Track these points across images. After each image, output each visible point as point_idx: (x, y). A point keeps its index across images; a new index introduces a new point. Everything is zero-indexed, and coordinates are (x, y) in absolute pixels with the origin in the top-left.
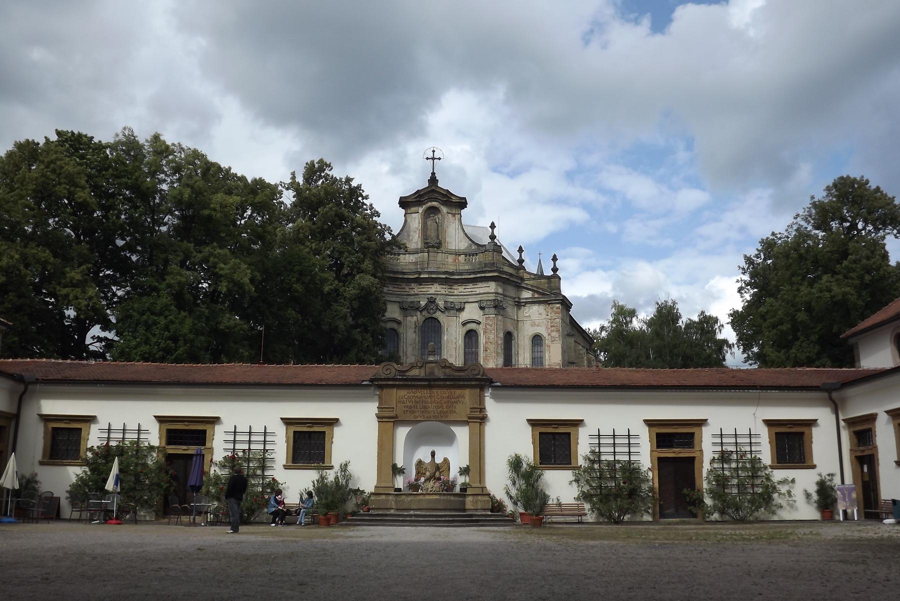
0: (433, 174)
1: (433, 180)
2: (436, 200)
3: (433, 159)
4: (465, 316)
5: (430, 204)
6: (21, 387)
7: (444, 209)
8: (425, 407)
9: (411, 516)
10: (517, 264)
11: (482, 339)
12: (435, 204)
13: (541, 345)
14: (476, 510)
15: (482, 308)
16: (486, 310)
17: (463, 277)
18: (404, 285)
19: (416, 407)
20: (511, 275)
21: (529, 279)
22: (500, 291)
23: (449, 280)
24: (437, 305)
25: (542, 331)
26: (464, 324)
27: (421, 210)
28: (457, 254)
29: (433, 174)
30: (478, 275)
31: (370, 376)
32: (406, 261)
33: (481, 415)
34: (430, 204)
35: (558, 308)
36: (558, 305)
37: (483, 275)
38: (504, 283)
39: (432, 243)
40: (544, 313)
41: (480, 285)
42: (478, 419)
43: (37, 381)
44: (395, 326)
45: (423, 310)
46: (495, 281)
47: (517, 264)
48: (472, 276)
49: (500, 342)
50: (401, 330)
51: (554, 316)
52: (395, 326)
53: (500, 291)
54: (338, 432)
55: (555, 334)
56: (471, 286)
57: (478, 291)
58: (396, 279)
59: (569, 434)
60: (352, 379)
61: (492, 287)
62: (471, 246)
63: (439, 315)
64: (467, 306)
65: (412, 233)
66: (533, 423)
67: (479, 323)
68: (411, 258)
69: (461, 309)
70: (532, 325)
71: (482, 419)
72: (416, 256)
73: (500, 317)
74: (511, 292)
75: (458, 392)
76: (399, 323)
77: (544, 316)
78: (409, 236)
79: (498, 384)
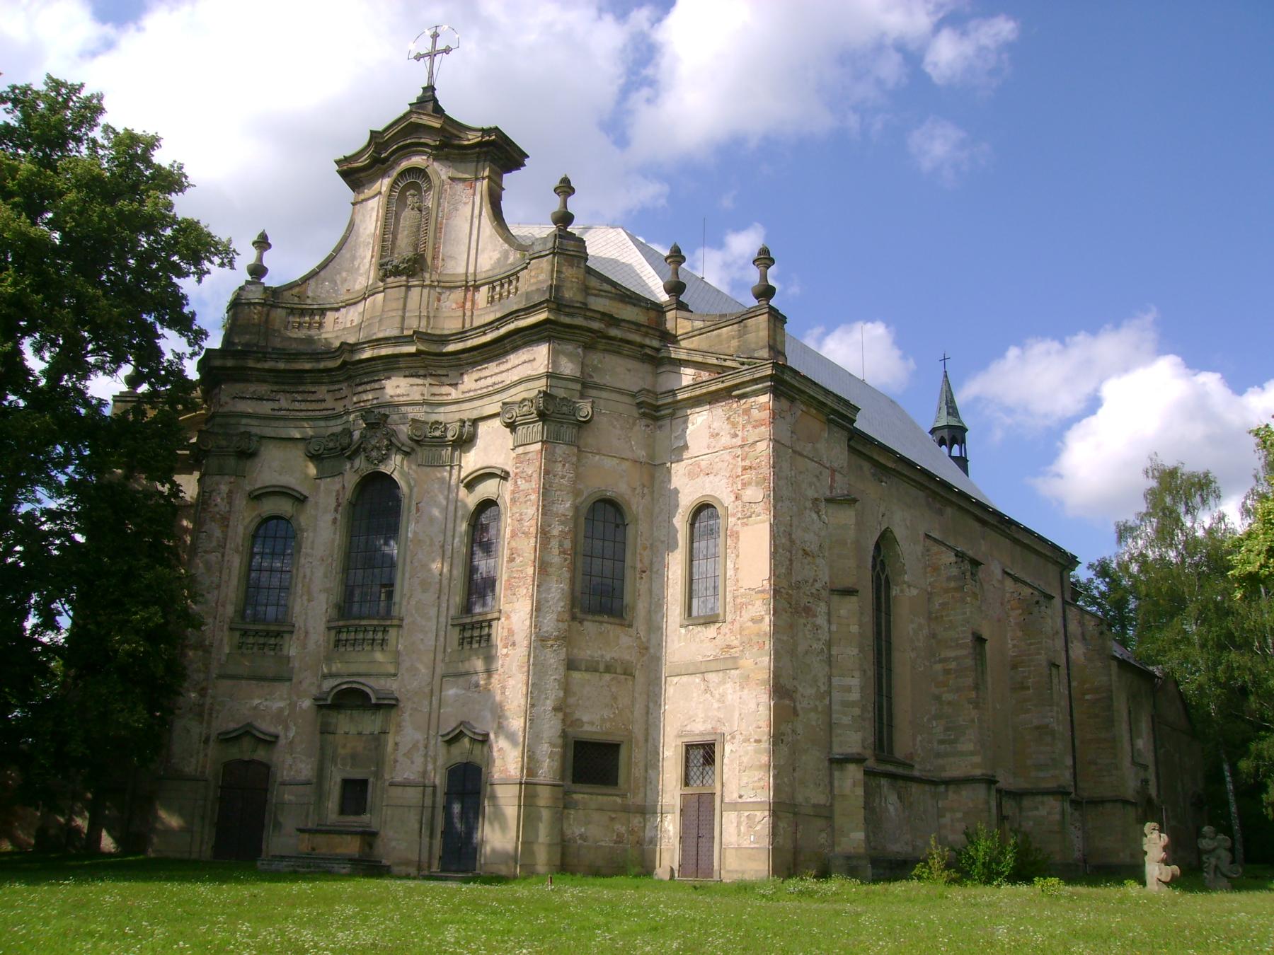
0: (430, 89)
3: (432, 55)
4: (471, 461)
5: (405, 164)
7: (440, 171)
10: (663, 297)
11: (507, 525)
12: (417, 161)
13: (712, 533)
15: (512, 426)
16: (521, 430)
17: (470, 344)
18: (322, 391)
21: (689, 336)
22: (568, 368)
23: (438, 358)
24: (391, 435)
25: (718, 488)
27: (384, 184)
28: (471, 286)
29: (430, 89)
30: (503, 331)
32: (340, 327)
34: (405, 164)
35: (761, 408)
36: (765, 398)
37: (511, 327)
38: (588, 347)
39: (407, 266)
41: (514, 359)
44: (284, 507)
45: (356, 453)
46: (548, 339)
47: (663, 297)
49: (556, 530)
50: (303, 520)
51: (753, 435)
52: (284, 507)
53: (568, 368)
55: (755, 494)
56: (492, 367)
58: (298, 378)
61: (537, 359)
62: (506, 255)
63: (395, 466)
64: (483, 428)
65: (361, 252)
67: (505, 476)
68: (352, 316)
69: (465, 441)
70: (692, 475)
72: (360, 307)
73: (561, 450)
74: (623, 374)
76: (300, 500)
77: (725, 440)
78: (354, 258)
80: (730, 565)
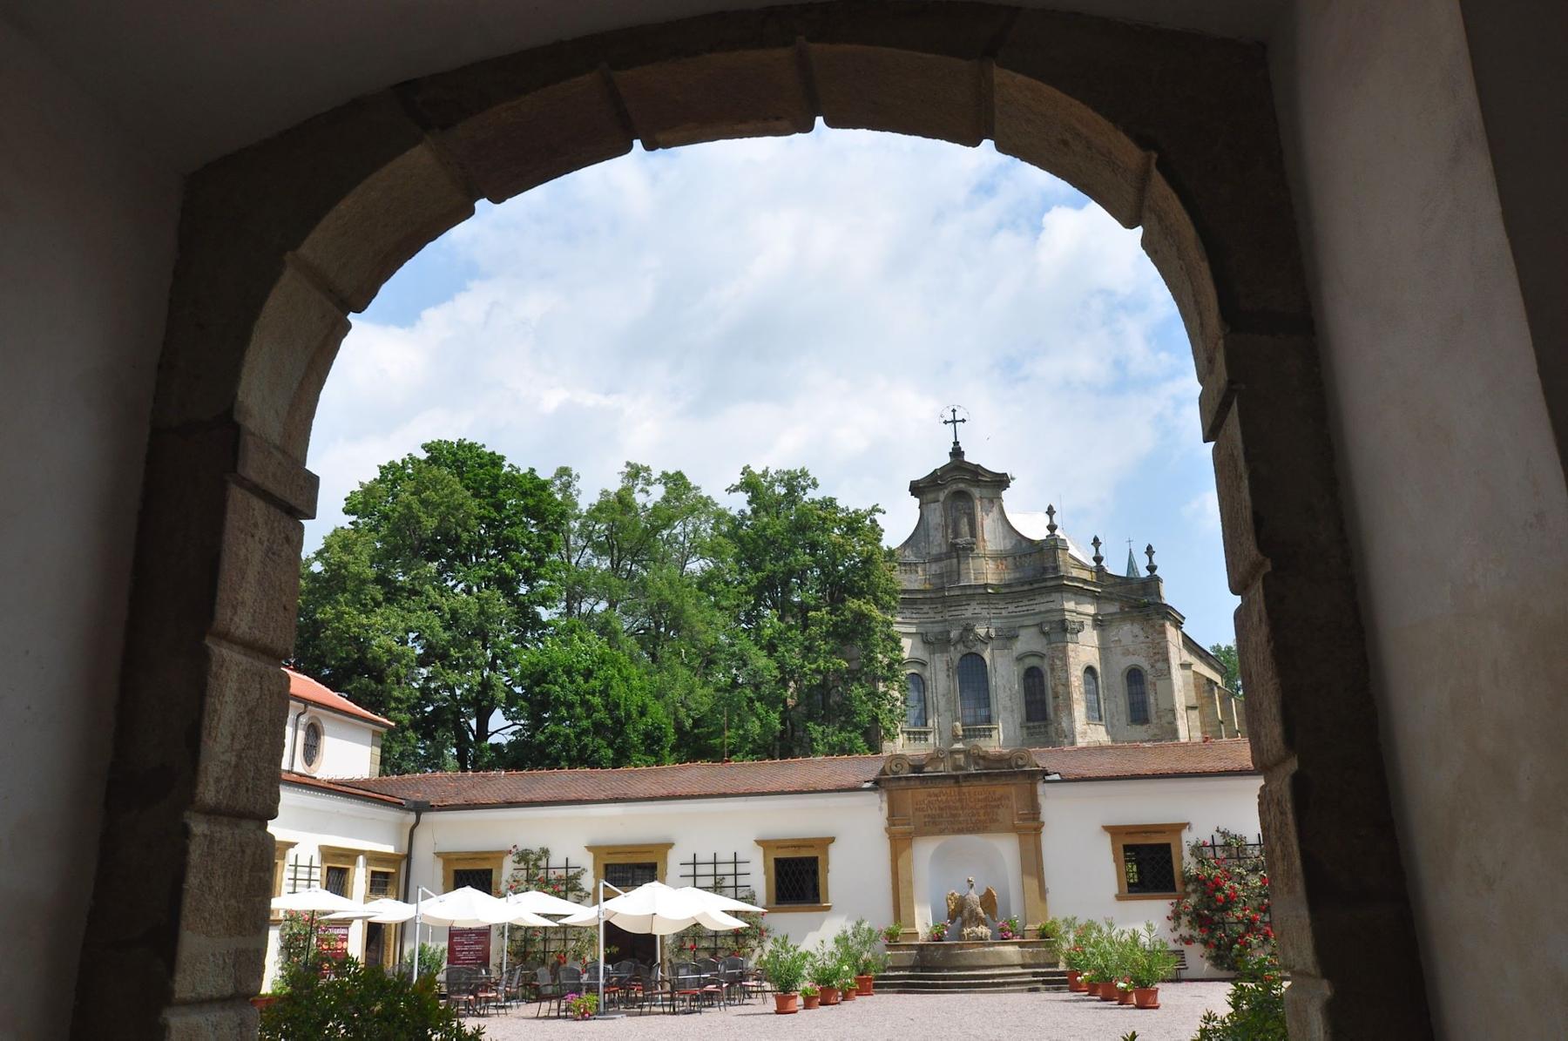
0: (956, 443)
1: (957, 452)
2: (962, 480)
3: (954, 422)
4: (1020, 646)
6: (412, 817)
7: (976, 492)
8: (954, 816)
9: (944, 978)
12: (962, 486)
14: (1039, 966)
15: (1044, 634)
16: (1053, 637)
18: (926, 608)
19: (941, 816)
20: (1085, 581)
26: (1020, 659)
29: (956, 443)
31: (872, 776)
33: (1034, 824)
34: (955, 487)
40: (1141, 635)
42: (1030, 826)
43: (431, 808)
48: (1026, 588)
50: (927, 674)
54: (834, 851)
57: (1037, 609)
59: (1168, 845)
60: (851, 780)
63: (978, 648)
64: (1023, 633)
65: (932, 532)
66: (1114, 831)
67: (1041, 656)
71: (1038, 830)
72: (942, 564)
75: (999, 790)
77: (1142, 638)
79: (1057, 777)
80: (1152, 700)
